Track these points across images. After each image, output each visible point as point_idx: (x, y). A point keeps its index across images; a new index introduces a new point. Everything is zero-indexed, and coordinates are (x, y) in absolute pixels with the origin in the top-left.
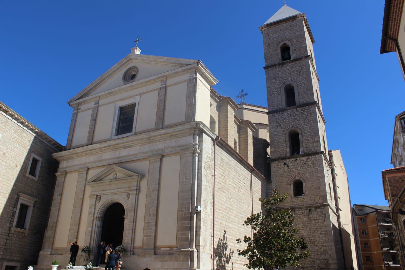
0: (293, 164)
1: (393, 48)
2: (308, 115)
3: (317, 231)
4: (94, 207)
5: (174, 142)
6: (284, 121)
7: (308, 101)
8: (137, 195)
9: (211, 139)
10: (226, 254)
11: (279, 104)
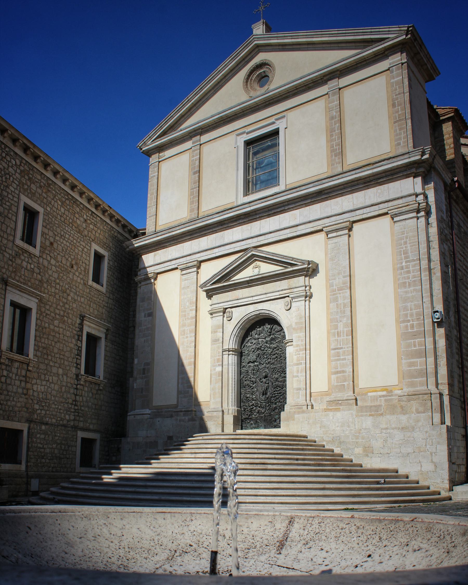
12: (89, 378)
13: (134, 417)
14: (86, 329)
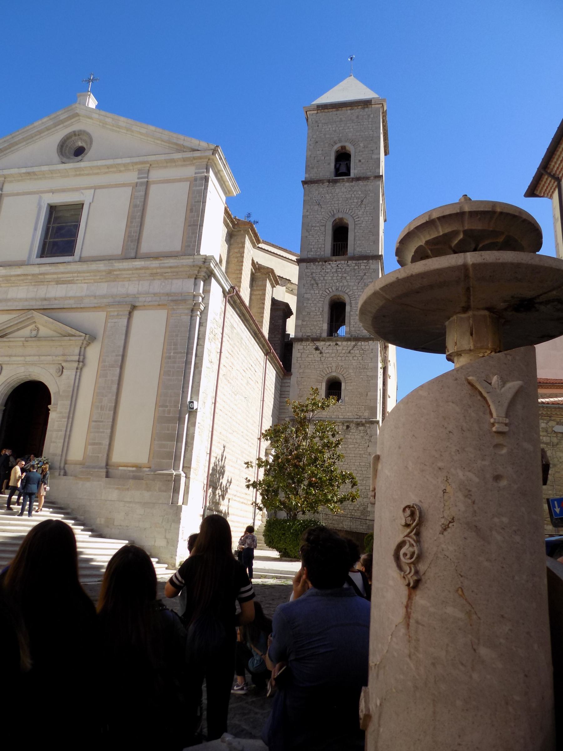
0: (331, 351)
1: (549, 192)
2: (365, 275)
3: (354, 461)
5: (157, 286)
6: (324, 279)
7: (369, 251)
8: (79, 371)
9: (221, 290)
10: (222, 483)
11: (320, 248)
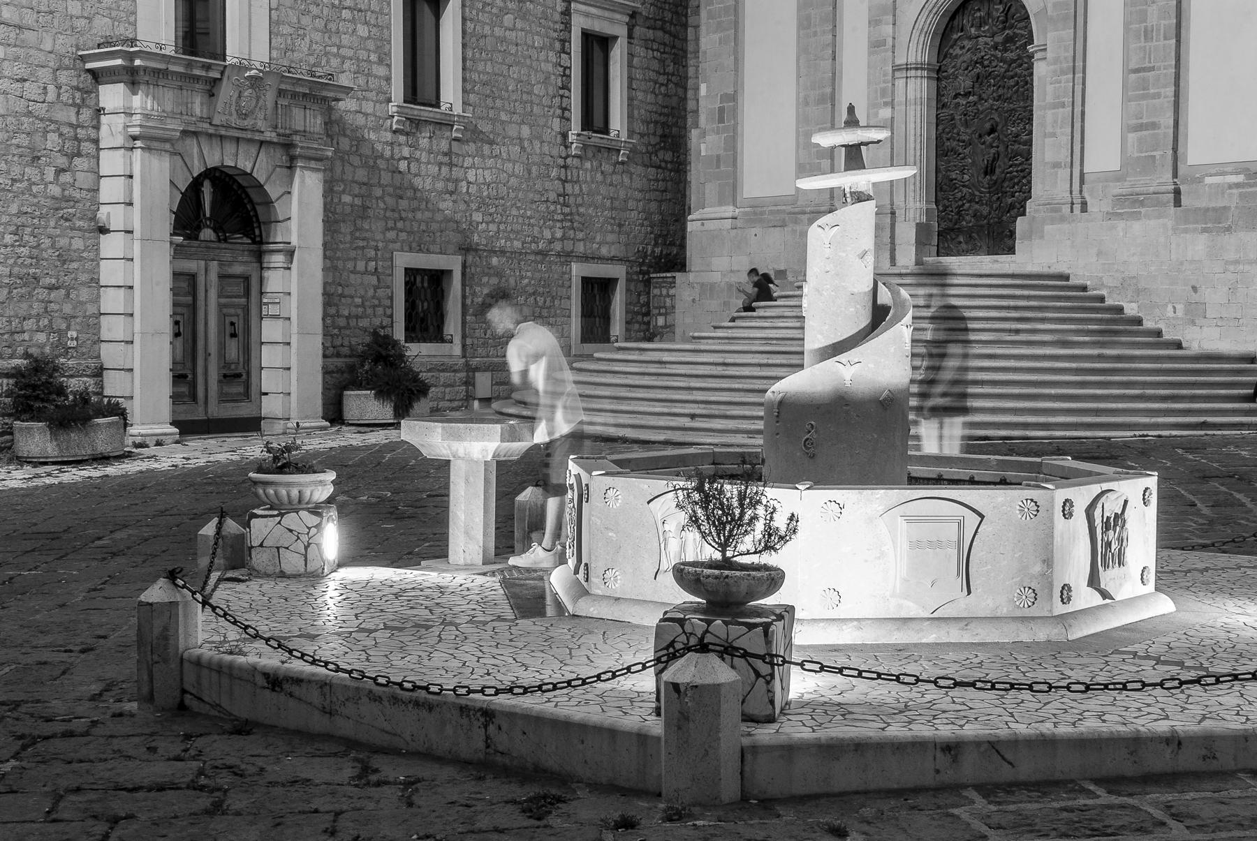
4: (890, 18)
12: (592, 140)
13: (703, 224)
14: (578, 23)
